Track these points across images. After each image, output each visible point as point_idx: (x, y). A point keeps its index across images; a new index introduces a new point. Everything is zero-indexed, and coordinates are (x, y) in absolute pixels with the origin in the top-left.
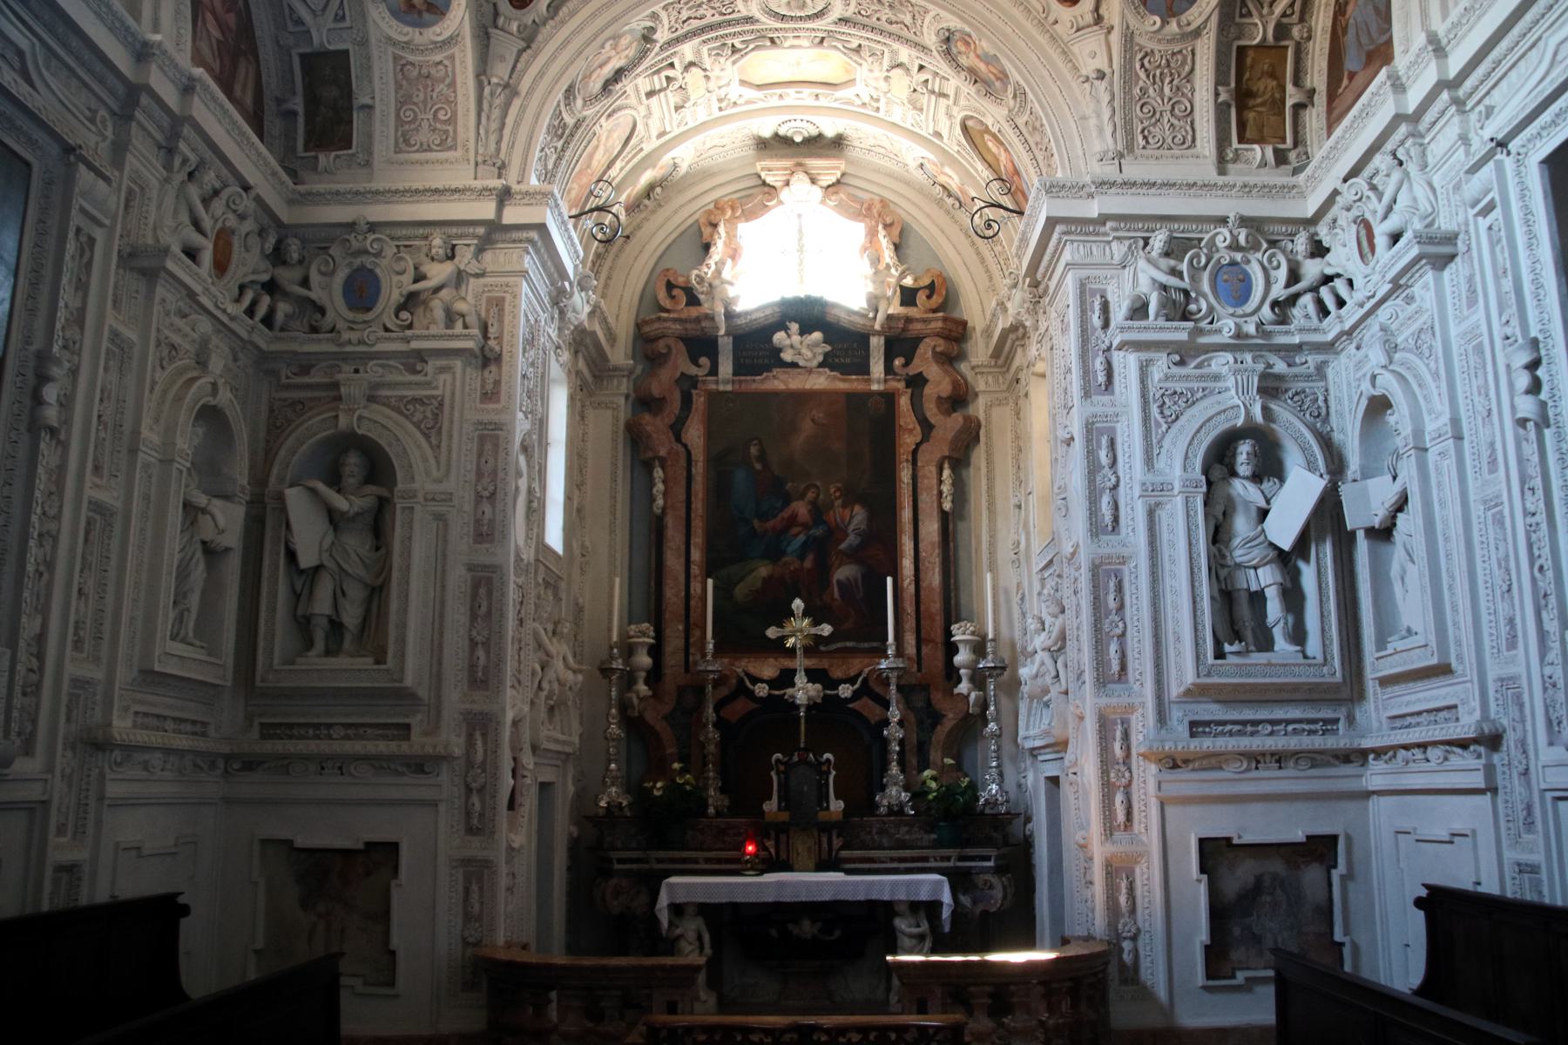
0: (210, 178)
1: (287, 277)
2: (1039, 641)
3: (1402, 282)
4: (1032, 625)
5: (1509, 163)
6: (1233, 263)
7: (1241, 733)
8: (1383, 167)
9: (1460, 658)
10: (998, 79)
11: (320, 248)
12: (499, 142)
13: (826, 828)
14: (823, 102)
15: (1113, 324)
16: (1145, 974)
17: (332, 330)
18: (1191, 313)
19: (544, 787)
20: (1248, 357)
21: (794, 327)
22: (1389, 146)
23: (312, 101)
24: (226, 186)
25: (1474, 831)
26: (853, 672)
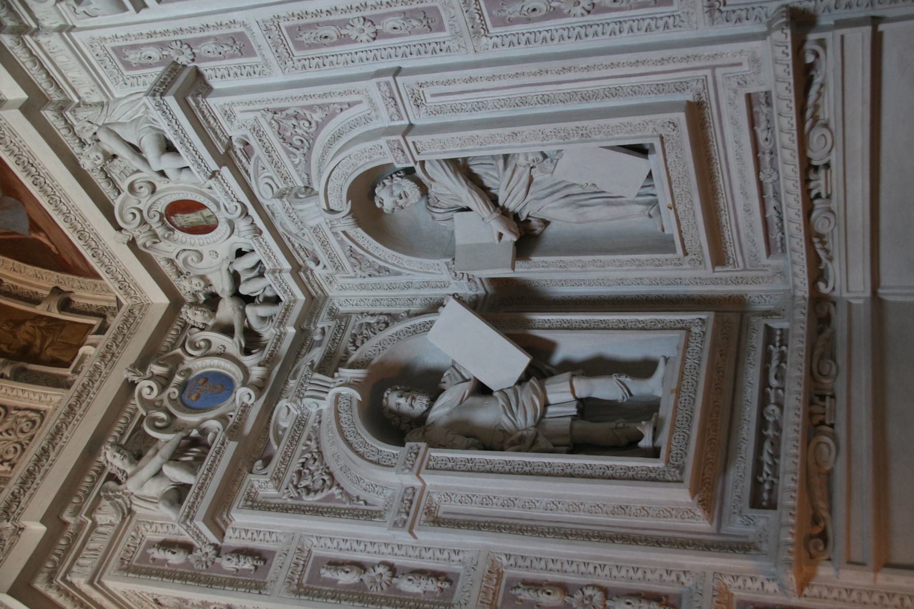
3: (222, 150)
6: (183, 387)
7: (776, 443)
9: (680, 87)
15: (187, 537)
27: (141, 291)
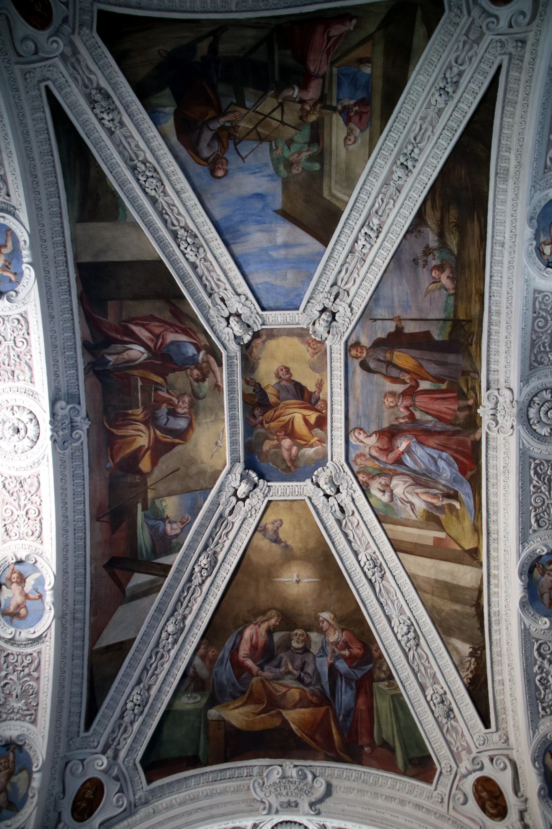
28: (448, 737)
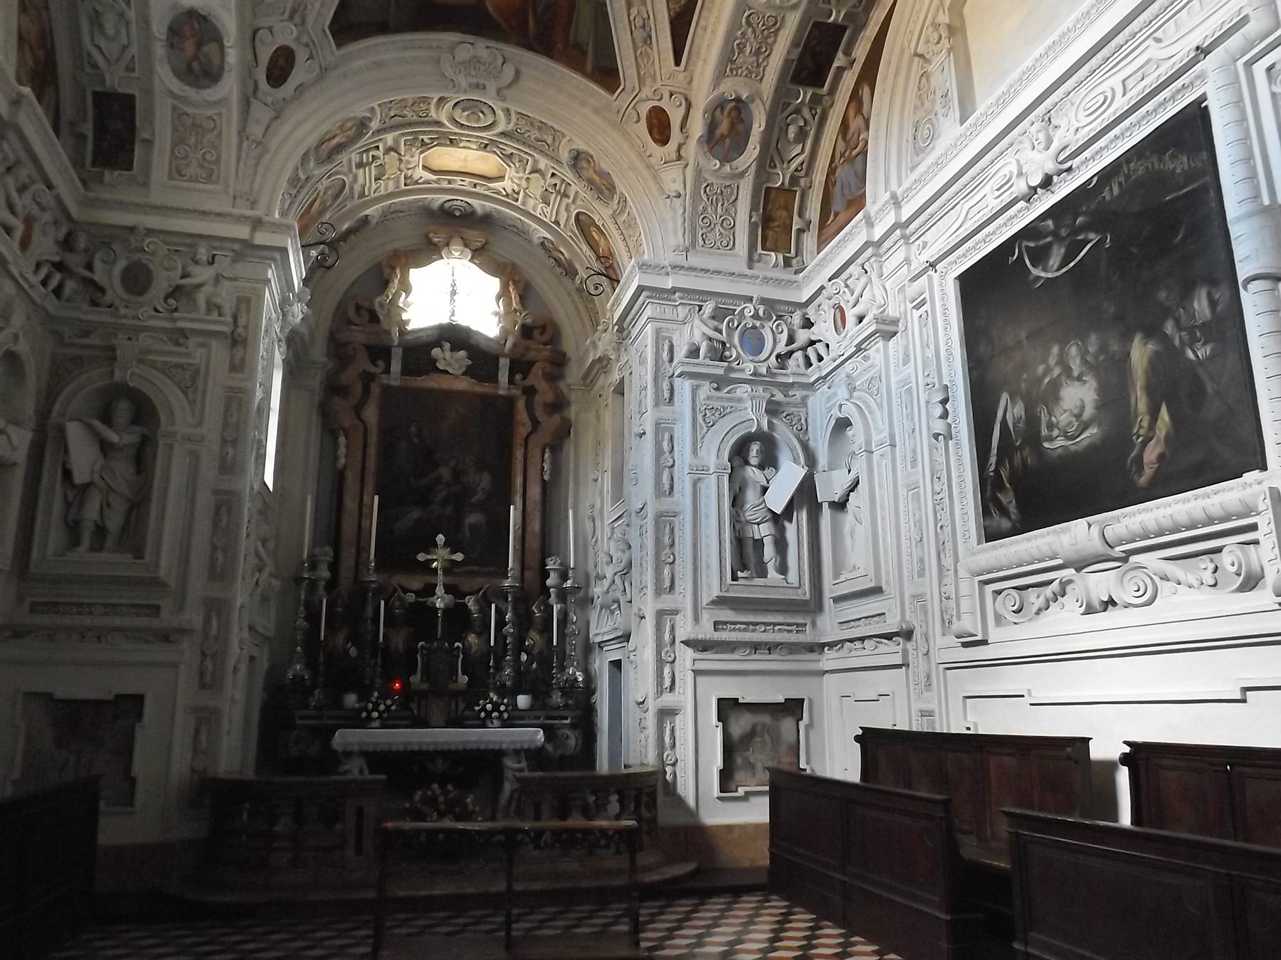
0: (25, 172)
1: (75, 261)
2: (609, 571)
3: (863, 347)
4: (602, 558)
5: (936, 277)
6: (754, 327)
7: (745, 630)
8: (856, 275)
10: (608, 189)
11: (103, 243)
12: (252, 183)
13: (456, 695)
14: (478, 190)
15: (676, 361)
16: (680, 790)
17: (110, 307)
18: (725, 357)
19: (252, 658)
20: (761, 389)
21: (447, 346)
22: (860, 261)
23: (100, 128)
24: (33, 182)
25: (893, 693)
26: (476, 588)
27: (807, 285)
28: (640, 61)
